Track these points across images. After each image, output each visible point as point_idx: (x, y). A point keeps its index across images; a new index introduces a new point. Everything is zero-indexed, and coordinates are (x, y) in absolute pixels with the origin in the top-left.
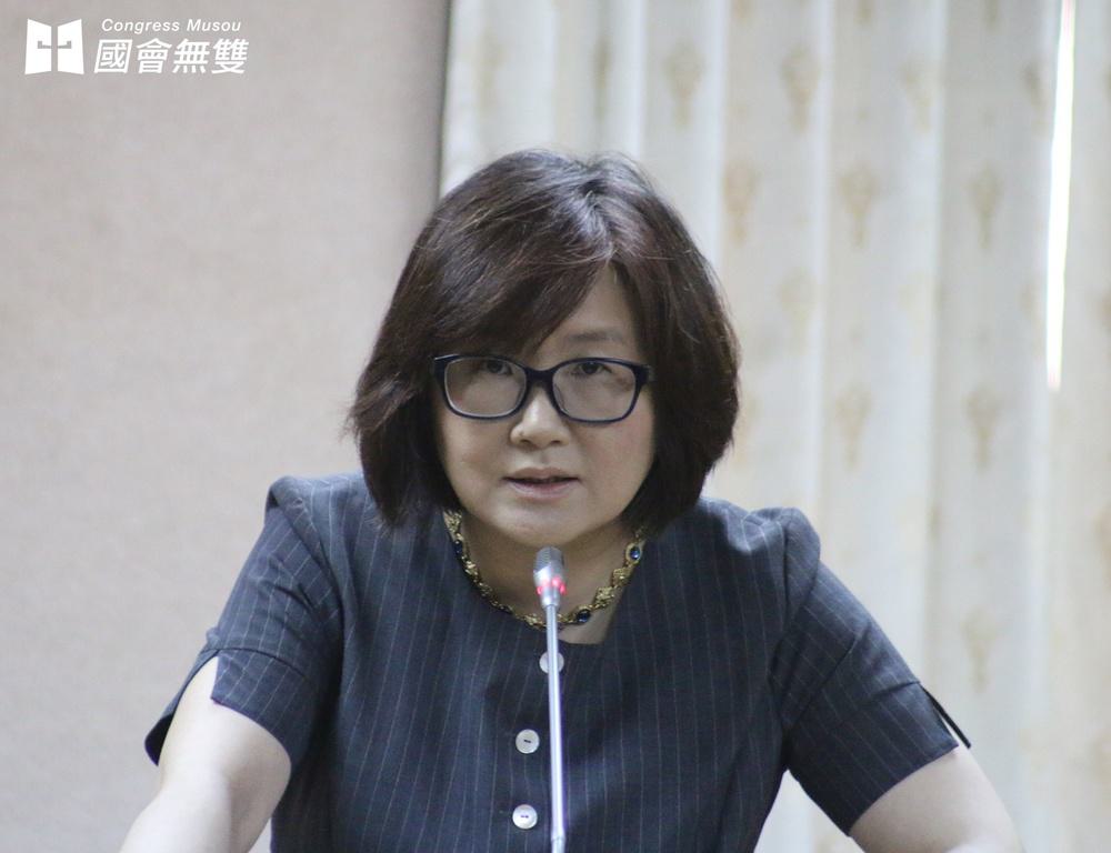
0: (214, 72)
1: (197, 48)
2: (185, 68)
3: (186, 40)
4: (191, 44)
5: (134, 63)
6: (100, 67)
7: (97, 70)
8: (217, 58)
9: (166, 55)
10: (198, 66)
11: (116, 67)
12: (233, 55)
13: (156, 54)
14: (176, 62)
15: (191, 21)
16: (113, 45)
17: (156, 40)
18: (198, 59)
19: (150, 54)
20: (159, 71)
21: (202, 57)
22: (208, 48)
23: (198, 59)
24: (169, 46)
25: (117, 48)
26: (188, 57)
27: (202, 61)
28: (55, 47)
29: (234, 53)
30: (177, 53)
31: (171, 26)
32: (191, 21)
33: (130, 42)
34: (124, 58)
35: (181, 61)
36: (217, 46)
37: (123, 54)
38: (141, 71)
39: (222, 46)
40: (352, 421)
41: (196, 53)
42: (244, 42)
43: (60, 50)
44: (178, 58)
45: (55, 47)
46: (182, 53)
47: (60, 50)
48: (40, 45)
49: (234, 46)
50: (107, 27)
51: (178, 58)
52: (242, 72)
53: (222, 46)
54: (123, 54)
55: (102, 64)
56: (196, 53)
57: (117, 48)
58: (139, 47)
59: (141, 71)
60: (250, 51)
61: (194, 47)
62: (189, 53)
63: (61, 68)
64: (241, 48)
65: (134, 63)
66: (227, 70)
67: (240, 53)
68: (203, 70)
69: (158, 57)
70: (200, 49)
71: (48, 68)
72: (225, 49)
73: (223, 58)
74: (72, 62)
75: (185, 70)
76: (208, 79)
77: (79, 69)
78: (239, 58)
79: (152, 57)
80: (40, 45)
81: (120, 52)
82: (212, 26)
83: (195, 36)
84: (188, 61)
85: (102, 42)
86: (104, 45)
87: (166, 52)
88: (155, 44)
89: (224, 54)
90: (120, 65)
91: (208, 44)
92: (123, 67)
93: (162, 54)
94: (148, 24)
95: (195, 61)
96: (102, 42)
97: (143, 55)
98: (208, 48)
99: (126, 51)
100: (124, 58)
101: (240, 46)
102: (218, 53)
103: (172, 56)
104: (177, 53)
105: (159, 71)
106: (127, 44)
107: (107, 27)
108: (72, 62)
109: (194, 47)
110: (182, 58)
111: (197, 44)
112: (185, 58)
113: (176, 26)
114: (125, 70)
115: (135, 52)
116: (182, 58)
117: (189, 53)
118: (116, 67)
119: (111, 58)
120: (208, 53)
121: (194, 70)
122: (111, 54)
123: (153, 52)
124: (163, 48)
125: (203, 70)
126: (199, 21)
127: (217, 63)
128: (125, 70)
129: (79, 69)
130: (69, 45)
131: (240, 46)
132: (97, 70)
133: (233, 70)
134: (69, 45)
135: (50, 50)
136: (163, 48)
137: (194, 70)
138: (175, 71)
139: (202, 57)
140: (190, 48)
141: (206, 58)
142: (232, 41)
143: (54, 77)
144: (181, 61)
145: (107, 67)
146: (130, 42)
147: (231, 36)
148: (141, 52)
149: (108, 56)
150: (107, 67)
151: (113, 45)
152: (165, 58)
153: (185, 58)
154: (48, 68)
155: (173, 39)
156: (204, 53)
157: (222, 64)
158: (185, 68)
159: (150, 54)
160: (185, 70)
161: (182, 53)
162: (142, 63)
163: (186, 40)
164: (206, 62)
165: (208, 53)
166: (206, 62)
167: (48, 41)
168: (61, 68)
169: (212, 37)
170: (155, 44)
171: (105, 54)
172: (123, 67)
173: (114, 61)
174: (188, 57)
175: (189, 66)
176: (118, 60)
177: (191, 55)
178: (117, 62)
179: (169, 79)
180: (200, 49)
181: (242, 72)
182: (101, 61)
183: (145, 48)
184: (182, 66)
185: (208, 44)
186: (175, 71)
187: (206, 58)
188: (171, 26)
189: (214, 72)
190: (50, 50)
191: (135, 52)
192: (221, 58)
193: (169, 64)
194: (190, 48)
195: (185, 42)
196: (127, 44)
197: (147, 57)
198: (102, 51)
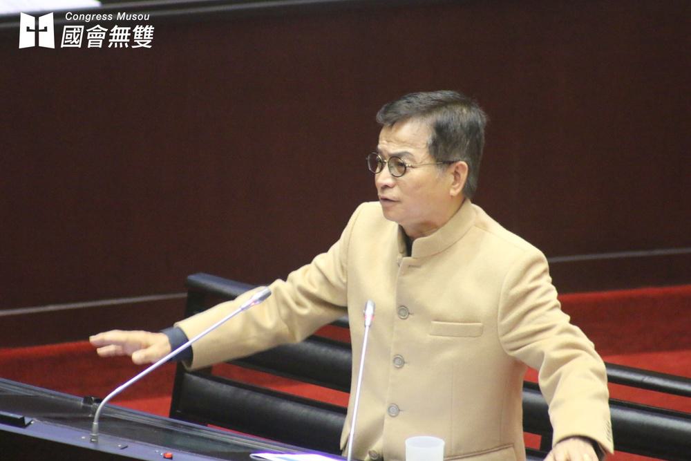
0: (133, 47)
1: (123, 31)
2: (116, 44)
3: (116, 26)
4: (119, 29)
5: (85, 41)
6: (64, 44)
7: (62, 46)
8: (135, 38)
9: (104, 36)
10: (124, 43)
11: (74, 44)
12: (144, 36)
13: (98, 35)
14: (110, 40)
15: (119, 14)
16: (73, 29)
17: (98, 26)
18: (124, 38)
19: (94, 35)
20: (100, 46)
21: (126, 37)
22: (129, 31)
23: (124, 38)
24: (106, 30)
25: (75, 31)
26: (118, 37)
27: (126, 40)
28: (37, 31)
29: (145, 35)
30: (111, 34)
31: (107, 17)
32: (119, 14)
33: (82, 27)
34: (79, 38)
35: (113, 40)
36: (135, 30)
37: (78, 35)
38: (89, 46)
39: (138, 30)
40: (428, 154)
41: (122, 34)
42: (151, 28)
43: (40, 33)
44: (111, 37)
45: (37, 31)
46: (114, 35)
47: (40, 33)
48: (28, 29)
49: (145, 30)
50: (68, 18)
51: (111, 37)
52: (150, 47)
53: (138, 30)
54: (78, 35)
55: (66, 42)
56: (122, 34)
57: (75, 31)
58: (88, 30)
59: (89, 46)
60: (155, 34)
61: (121, 31)
62: (118, 34)
63: (40, 45)
64: (150, 31)
65: (85, 41)
66: (141, 45)
67: (149, 35)
68: (127, 45)
69: (100, 37)
70: (125, 32)
71: (33, 45)
72: (140, 32)
73: (139, 38)
74: (47, 41)
75: (116, 46)
76: (129, 53)
77: (53, 47)
78: (149, 38)
79: (96, 37)
80: (28, 29)
81: (76, 34)
82: (132, 17)
83: (122, 23)
84: (118, 40)
85: (65, 27)
86: (67, 29)
87: (104, 34)
88: (98, 28)
89: (140, 35)
90: (77, 42)
91: (130, 28)
92: (78, 44)
93: (102, 35)
94: (93, 16)
95: (122, 40)
96: (65, 27)
97: (91, 36)
98: (129, 31)
99: (80, 33)
100: (79, 36)
101: (149, 30)
102: (136, 35)
103: (108, 37)
104: (111, 34)
105: (100, 46)
106: (81, 29)
107: (68, 18)
108: (47, 41)
109: (121, 31)
110: (114, 37)
111: (123, 29)
112: (116, 38)
113: (110, 17)
114: (79, 46)
115: (85, 34)
116: (114, 37)
117: (118, 34)
118: (74, 44)
119: (71, 38)
120: (130, 34)
121: (121, 46)
122: (71, 35)
123: (96, 34)
124: (103, 31)
125: (127, 45)
126: (124, 13)
127: (135, 41)
128: (79, 46)
129: (53, 47)
130: (45, 30)
131: (149, 30)
132: (62, 46)
133: (145, 45)
134: (45, 30)
135: (34, 33)
136: (103, 31)
137: (121, 46)
138: (110, 46)
139: (126, 37)
140: (119, 31)
141: (129, 37)
142: (144, 27)
143: (37, 48)
144: (113, 40)
145: (69, 43)
146: (82, 27)
147: (144, 23)
148: (89, 34)
149: (69, 36)
150: (69, 43)
151: (73, 29)
152: (103, 38)
153: (116, 38)
154: (33, 45)
155: (109, 25)
156: (127, 34)
157: (138, 42)
158: (116, 44)
159: (94, 35)
160: (116, 46)
161: (114, 35)
162: (90, 41)
163: (116, 26)
164: (128, 40)
165: (130, 34)
166: (128, 40)
167: (33, 27)
168: (40, 45)
169: (132, 24)
170: (98, 28)
171: (67, 35)
172: (78, 44)
173: (73, 39)
174: (118, 37)
175: (118, 43)
176: (75, 39)
177: (120, 36)
178: (75, 41)
179: (107, 52)
180: (125, 32)
181: (150, 47)
182: (65, 40)
183: (92, 31)
184: (114, 43)
185: (130, 28)
186: (110, 46)
187: (129, 37)
188: (107, 17)
189: (133, 47)
190: (34, 33)
191: (85, 34)
192: (137, 37)
193: (106, 42)
194: (119, 31)
195: (116, 28)
196: (81, 29)
197: (93, 37)
198: (66, 33)
